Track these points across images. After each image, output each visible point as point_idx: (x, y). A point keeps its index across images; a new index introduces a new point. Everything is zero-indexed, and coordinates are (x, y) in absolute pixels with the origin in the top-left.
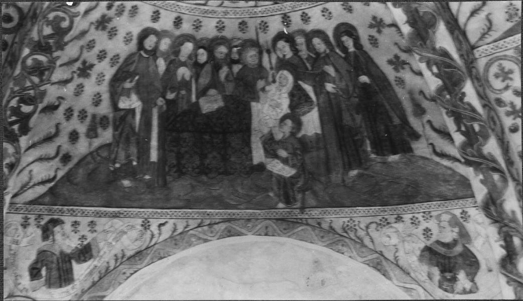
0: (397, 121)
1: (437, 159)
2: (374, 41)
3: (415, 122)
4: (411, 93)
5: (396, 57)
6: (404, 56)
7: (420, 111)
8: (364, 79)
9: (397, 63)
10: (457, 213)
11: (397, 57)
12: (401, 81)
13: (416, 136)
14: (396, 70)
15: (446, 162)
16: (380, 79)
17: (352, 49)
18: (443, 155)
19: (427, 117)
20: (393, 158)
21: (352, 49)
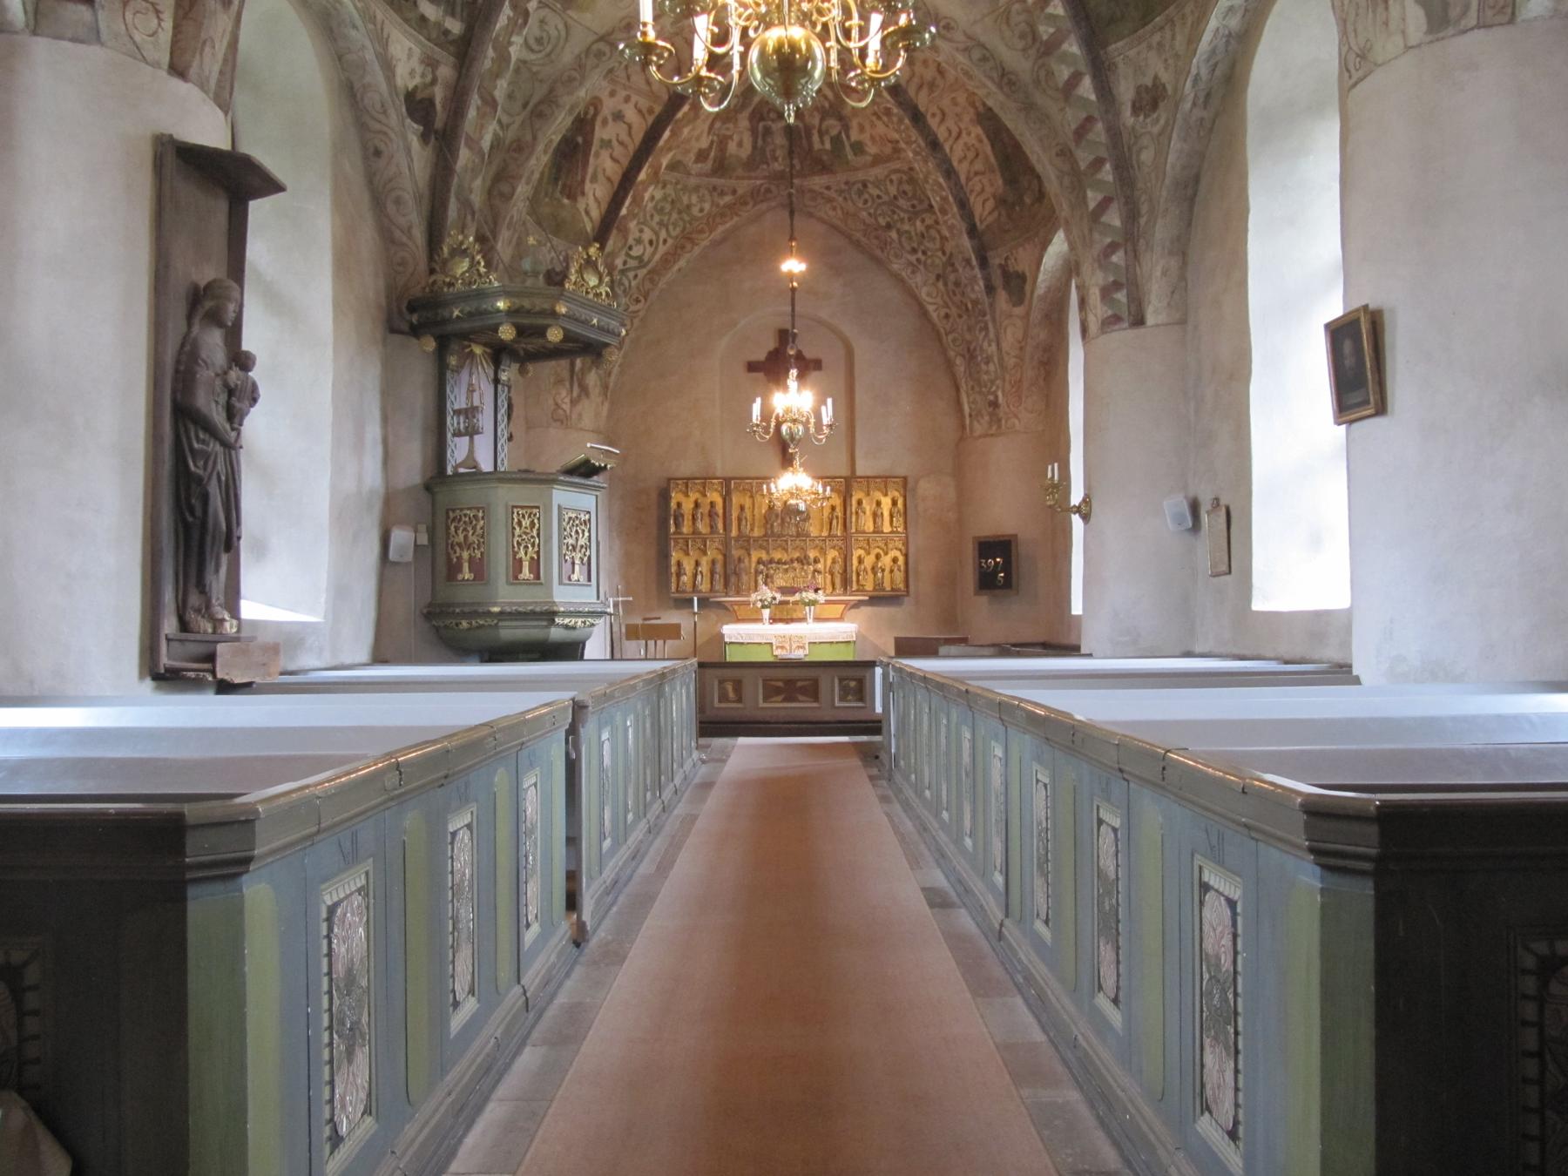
0: (579, 178)
1: (583, 213)
2: (605, 122)
3: (588, 185)
4: (596, 167)
5: (610, 141)
6: (615, 143)
7: (594, 179)
8: (580, 140)
9: (606, 144)
10: (570, 253)
11: (610, 141)
12: (597, 155)
13: (583, 194)
14: (601, 147)
15: (586, 219)
16: (588, 143)
17: (589, 116)
18: (587, 213)
19: (595, 186)
20: (566, 201)
21: (589, 116)
